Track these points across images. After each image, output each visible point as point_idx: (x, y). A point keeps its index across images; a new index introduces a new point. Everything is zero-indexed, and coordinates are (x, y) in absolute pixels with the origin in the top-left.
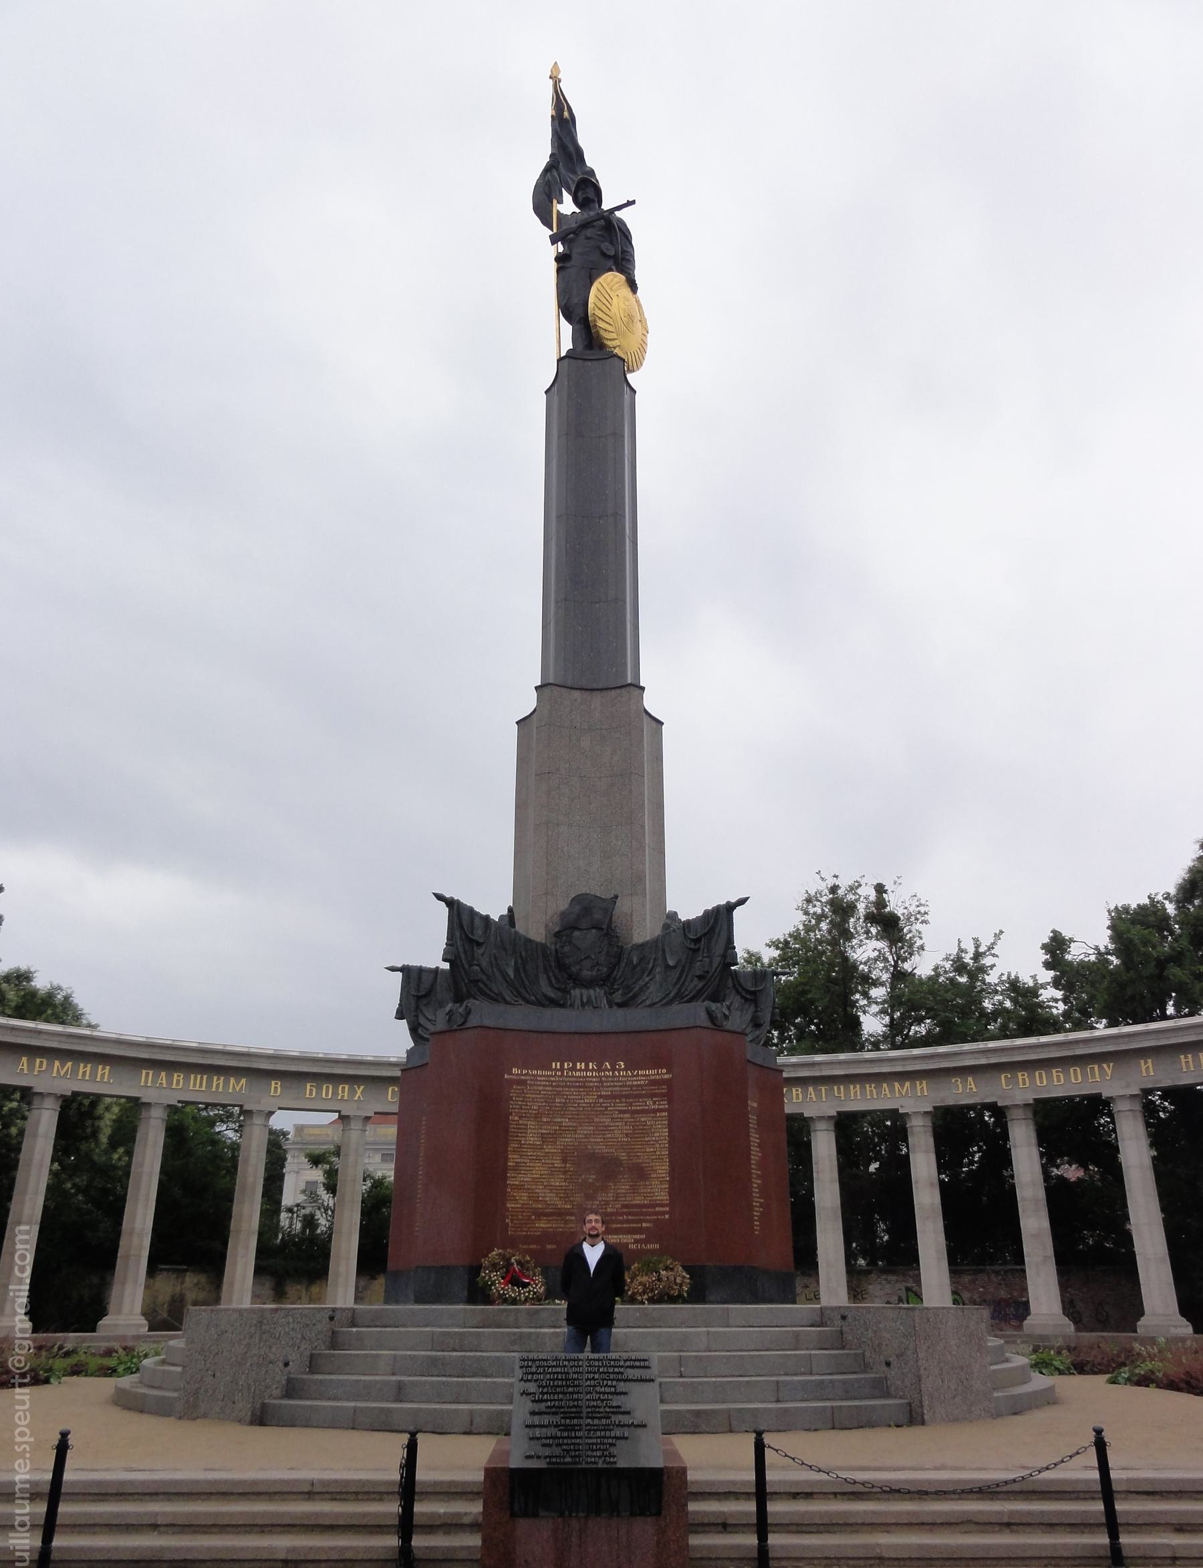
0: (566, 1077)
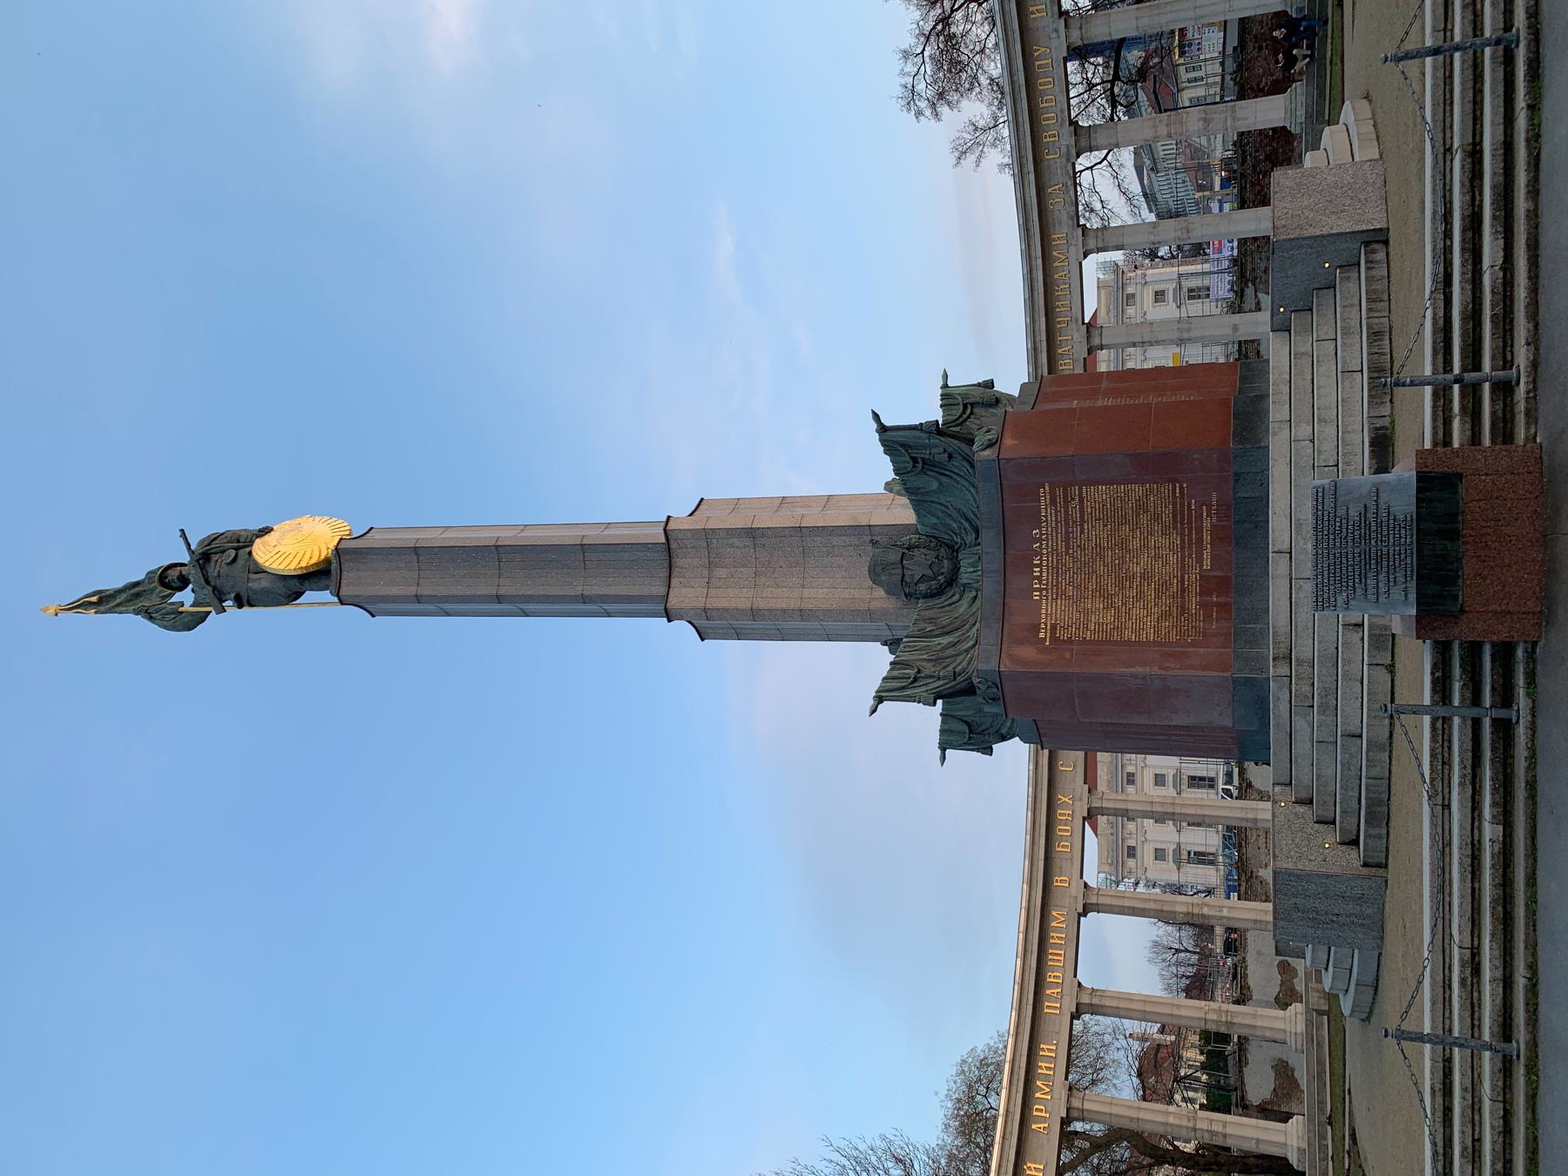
0: (1047, 585)
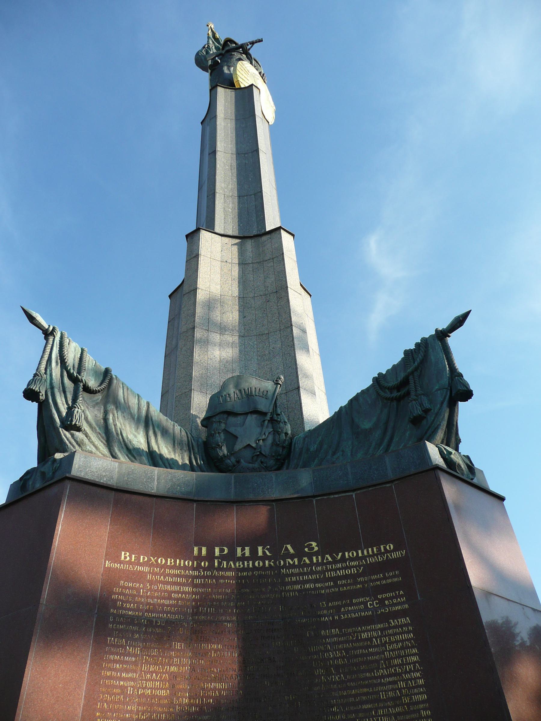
0: (219, 569)
